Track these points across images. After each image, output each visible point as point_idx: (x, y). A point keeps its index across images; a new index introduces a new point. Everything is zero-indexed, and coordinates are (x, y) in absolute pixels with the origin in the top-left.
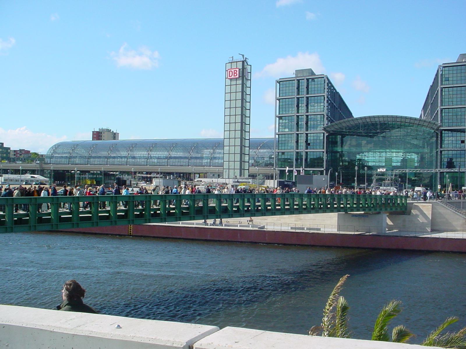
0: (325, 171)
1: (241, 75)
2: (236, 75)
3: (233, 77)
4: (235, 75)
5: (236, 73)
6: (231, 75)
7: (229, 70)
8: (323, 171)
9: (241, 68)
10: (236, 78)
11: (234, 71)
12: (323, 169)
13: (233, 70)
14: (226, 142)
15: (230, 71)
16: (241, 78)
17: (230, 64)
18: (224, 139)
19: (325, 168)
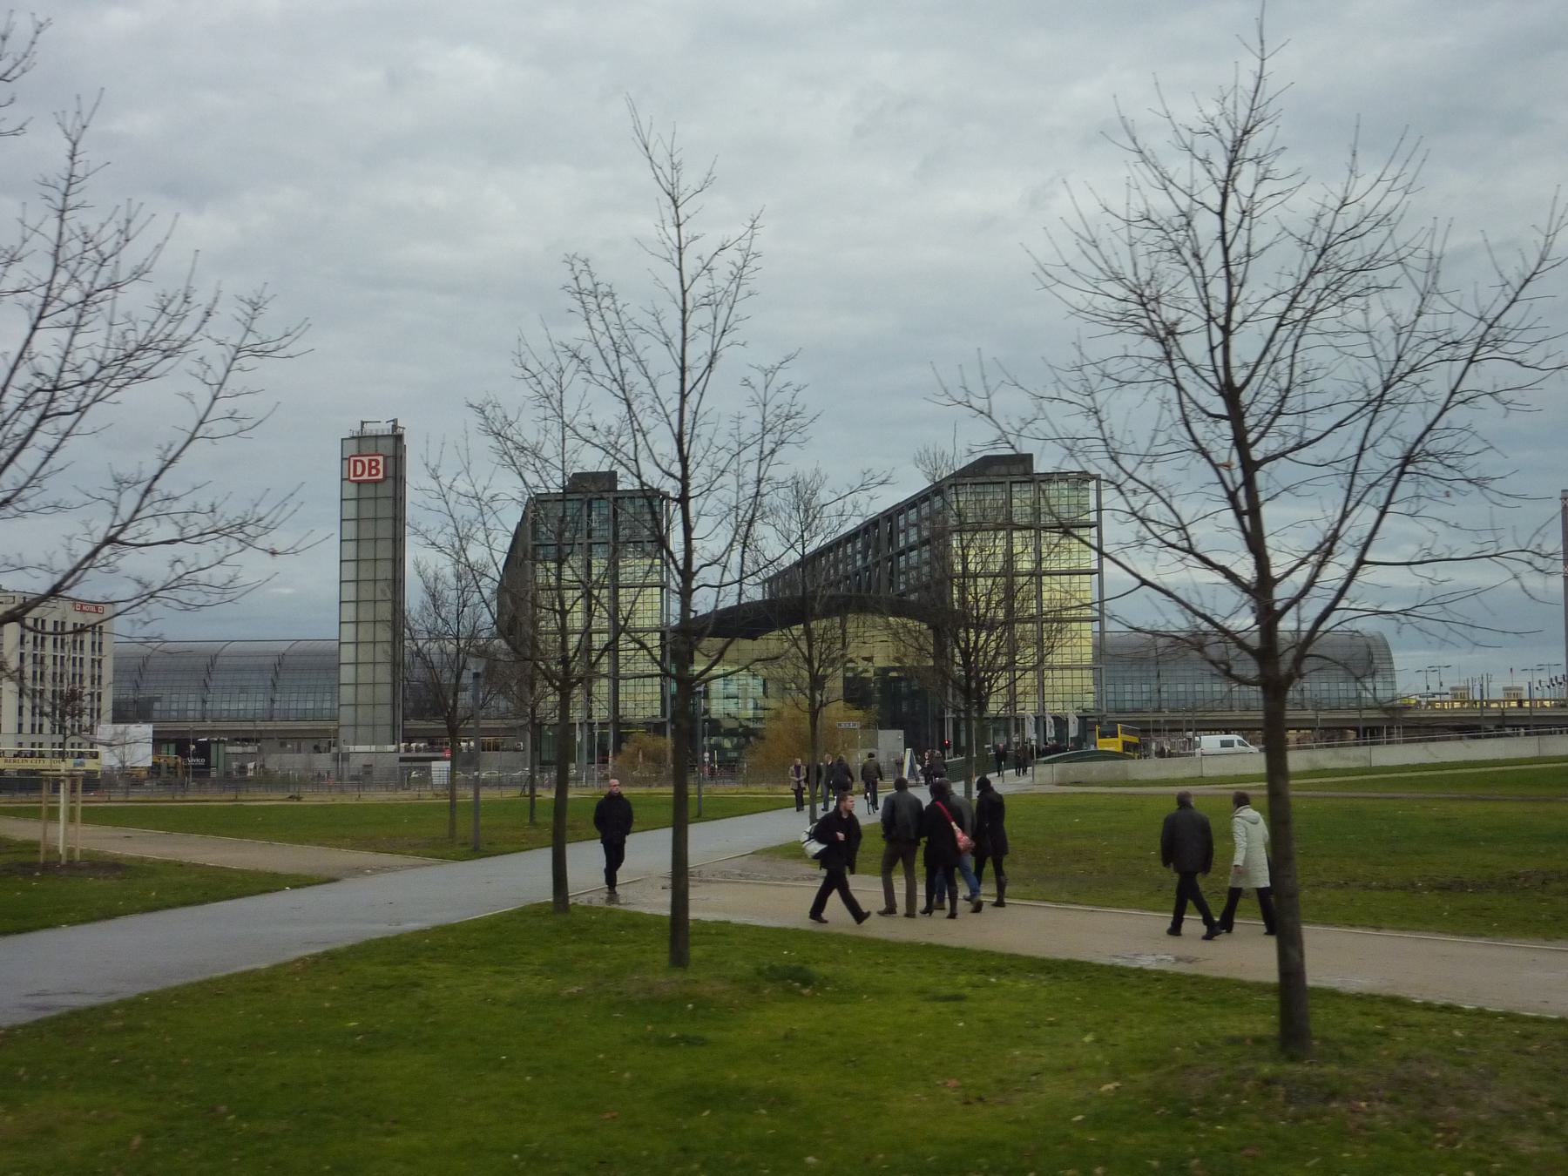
1: (390, 472)
2: (377, 474)
3: (366, 477)
4: (374, 471)
6: (359, 472)
7: (352, 459)
9: (390, 452)
10: (376, 482)
11: (370, 461)
12: (666, 720)
13: (366, 460)
14: (348, 653)
15: (355, 462)
16: (390, 482)
17: (355, 441)
19: (669, 715)
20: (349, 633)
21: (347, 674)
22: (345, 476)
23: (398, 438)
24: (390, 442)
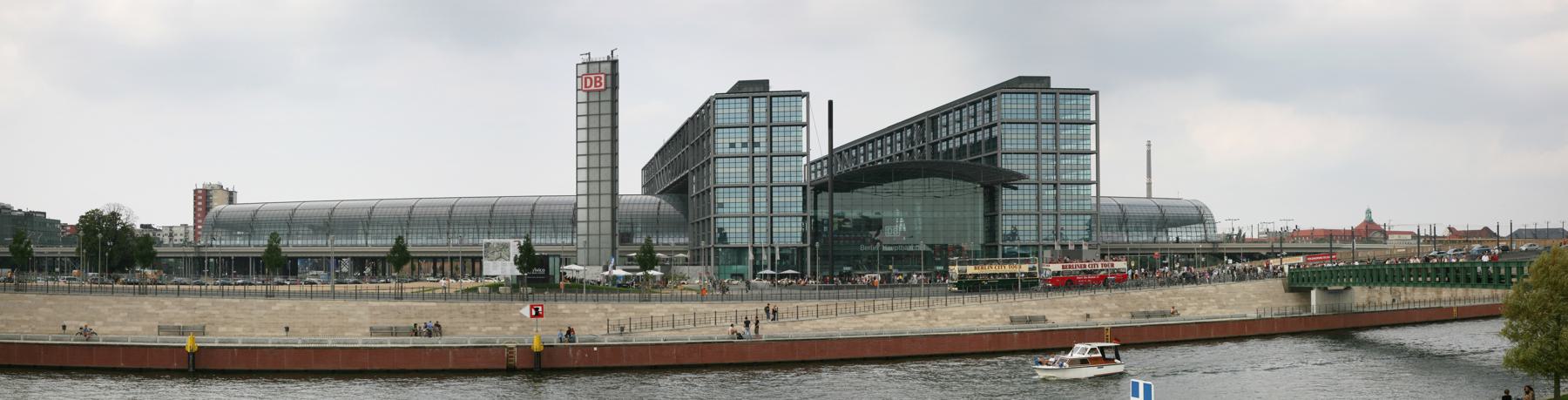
0: (809, 249)
1: (609, 85)
3: (593, 88)
4: (598, 84)
5: (599, 82)
6: (588, 84)
8: (806, 247)
9: (609, 72)
10: (600, 91)
11: (596, 78)
13: (593, 77)
14: (582, 202)
16: (609, 91)
17: (585, 66)
18: (577, 195)
20: (583, 188)
21: (582, 215)
22: (580, 88)
23: (614, 63)
24: (608, 66)
